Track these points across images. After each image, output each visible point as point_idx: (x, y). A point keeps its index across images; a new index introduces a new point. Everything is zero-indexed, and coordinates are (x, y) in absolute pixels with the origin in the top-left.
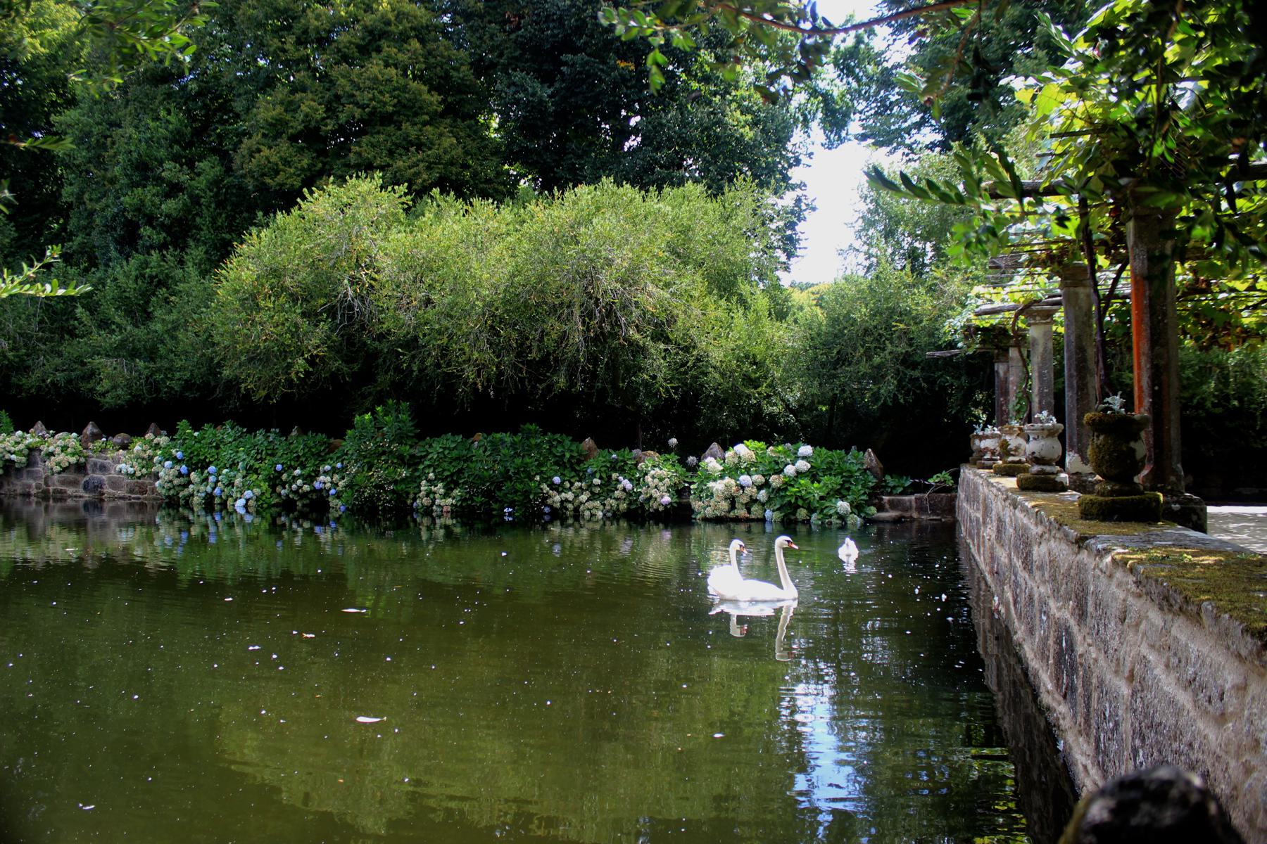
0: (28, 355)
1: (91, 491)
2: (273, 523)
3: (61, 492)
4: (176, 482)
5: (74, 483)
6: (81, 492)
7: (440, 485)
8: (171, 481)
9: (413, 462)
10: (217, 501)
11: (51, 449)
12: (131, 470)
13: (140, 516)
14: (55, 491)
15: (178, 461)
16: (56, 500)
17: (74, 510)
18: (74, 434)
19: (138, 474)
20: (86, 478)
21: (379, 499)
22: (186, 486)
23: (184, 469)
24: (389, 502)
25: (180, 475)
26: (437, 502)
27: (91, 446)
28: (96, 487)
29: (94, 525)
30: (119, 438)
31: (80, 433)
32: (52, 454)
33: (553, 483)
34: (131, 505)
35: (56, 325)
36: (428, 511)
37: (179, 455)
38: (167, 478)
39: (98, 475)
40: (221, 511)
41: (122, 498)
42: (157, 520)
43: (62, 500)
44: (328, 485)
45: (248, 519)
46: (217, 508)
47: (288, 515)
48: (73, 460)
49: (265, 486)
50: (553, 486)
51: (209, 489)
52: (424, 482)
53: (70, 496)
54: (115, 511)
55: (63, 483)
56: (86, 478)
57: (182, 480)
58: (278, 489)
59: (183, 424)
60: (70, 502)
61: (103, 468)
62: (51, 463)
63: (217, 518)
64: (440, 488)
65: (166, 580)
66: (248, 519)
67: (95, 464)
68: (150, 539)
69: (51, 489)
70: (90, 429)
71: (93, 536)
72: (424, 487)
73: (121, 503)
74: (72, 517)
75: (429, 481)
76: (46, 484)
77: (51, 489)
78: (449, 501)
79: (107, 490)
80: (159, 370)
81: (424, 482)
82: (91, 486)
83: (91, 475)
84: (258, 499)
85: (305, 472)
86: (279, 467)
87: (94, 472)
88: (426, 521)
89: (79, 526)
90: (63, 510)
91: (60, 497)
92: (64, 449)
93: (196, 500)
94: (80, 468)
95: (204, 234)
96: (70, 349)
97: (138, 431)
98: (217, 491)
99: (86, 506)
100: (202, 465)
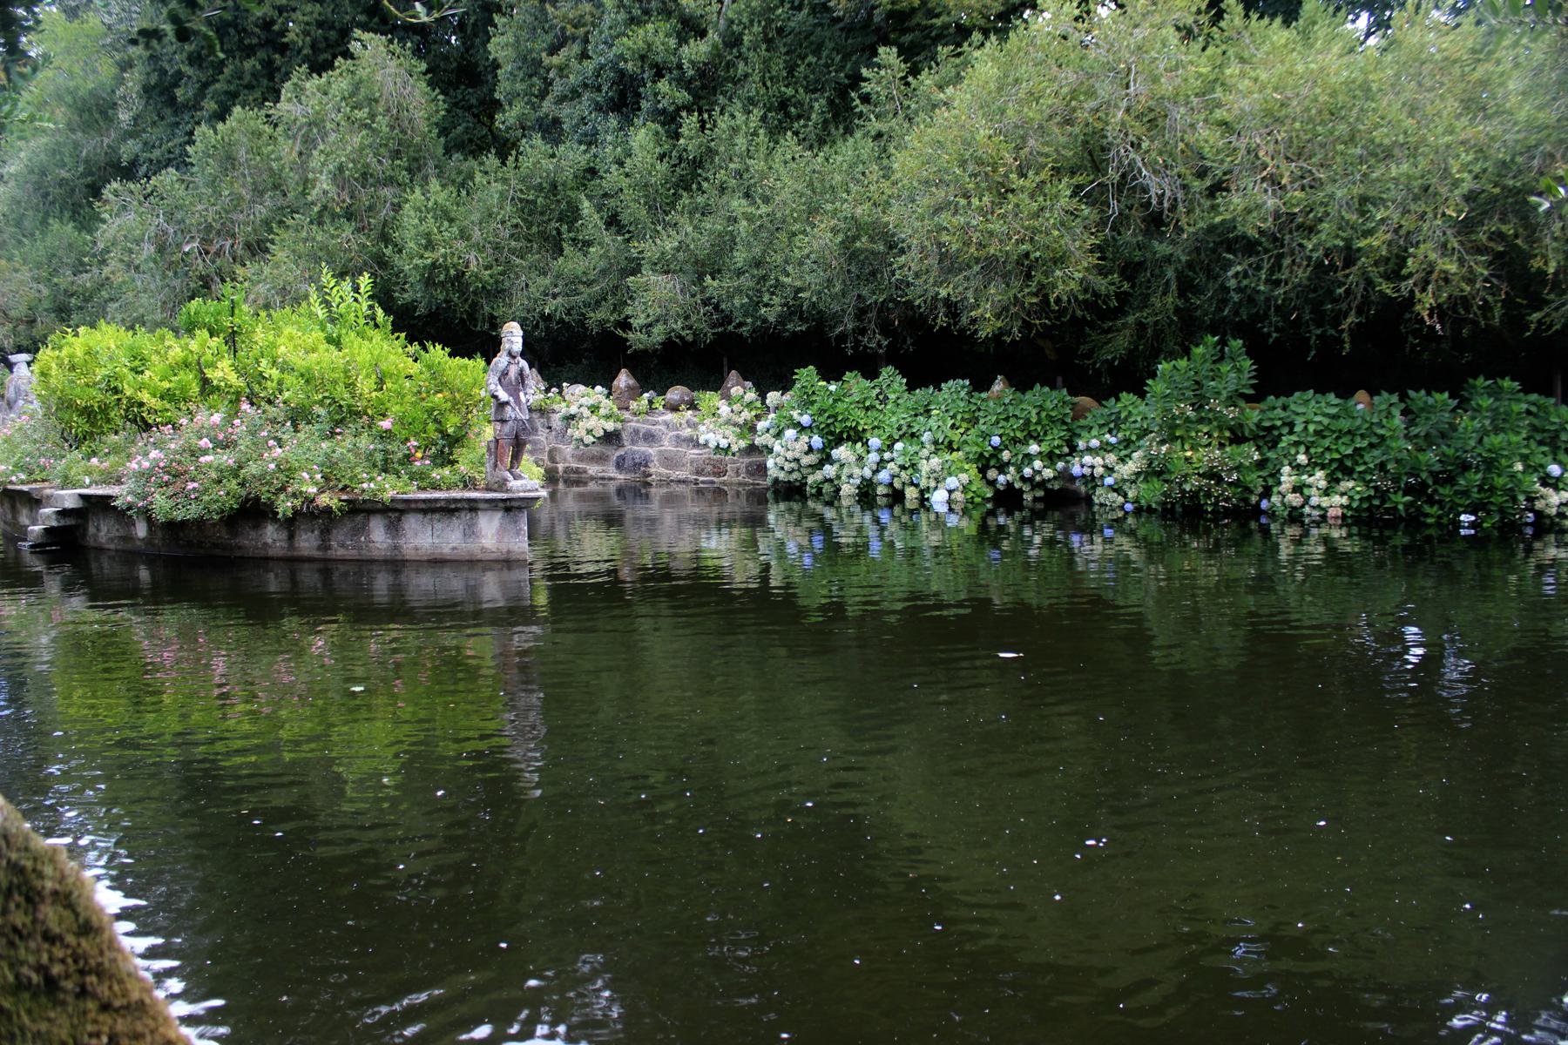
0: (503, 273)
1: (629, 471)
2: (983, 527)
3: (577, 471)
4: (806, 460)
5: (601, 459)
6: (612, 472)
7: (1320, 474)
8: (797, 460)
9: (1267, 437)
10: (881, 490)
11: (573, 410)
12: (724, 443)
13: (715, 510)
14: (566, 470)
15: (802, 428)
16: (569, 483)
17: (602, 497)
18: (599, 388)
19: (735, 448)
20: (621, 452)
21: (1208, 495)
22: (819, 465)
23: (817, 441)
24: (1227, 500)
25: (810, 450)
26: (1314, 501)
27: (633, 405)
28: (642, 464)
29: (637, 520)
30: (676, 393)
31: (609, 387)
32: (572, 417)
33: (1548, 475)
34: (699, 492)
35: (534, 229)
36: (1295, 516)
37: (805, 420)
38: (790, 455)
39: (642, 448)
40: (891, 507)
41: (679, 481)
42: (771, 517)
43: (578, 483)
44: (1099, 471)
45: (953, 521)
46: (881, 501)
47: (1009, 514)
48: (610, 426)
49: (973, 469)
50: (1546, 481)
51: (867, 473)
52: (1286, 469)
53: (592, 478)
54: (670, 500)
55: (581, 459)
56: (621, 452)
57: (812, 459)
58: (992, 474)
59: (807, 375)
60: (592, 487)
61: (650, 438)
62: (577, 432)
63: (885, 517)
64: (1319, 478)
65: (768, 608)
66: (953, 521)
67: (636, 432)
68: (753, 544)
69: (561, 467)
70: (623, 379)
71: (635, 535)
72: (1287, 478)
73: (681, 488)
74: (597, 508)
75: (1298, 468)
76: (552, 459)
77: (561, 467)
78: (1337, 500)
79: (657, 470)
80: (739, 290)
81: (1286, 469)
82: (628, 463)
83: (628, 447)
84: (965, 489)
85: (1045, 448)
86: (996, 440)
87: (633, 442)
88: (1293, 531)
89: (612, 520)
90: (582, 497)
91: (575, 479)
92: (594, 409)
93: (848, 489)
94: (611, 438)
95: (752, 88)
96: (572, 263)
97: (714, 382)
98: (883, 476)
99: (620, 492)
100: (856, 436)
